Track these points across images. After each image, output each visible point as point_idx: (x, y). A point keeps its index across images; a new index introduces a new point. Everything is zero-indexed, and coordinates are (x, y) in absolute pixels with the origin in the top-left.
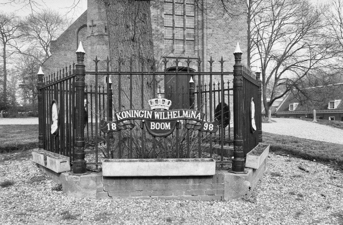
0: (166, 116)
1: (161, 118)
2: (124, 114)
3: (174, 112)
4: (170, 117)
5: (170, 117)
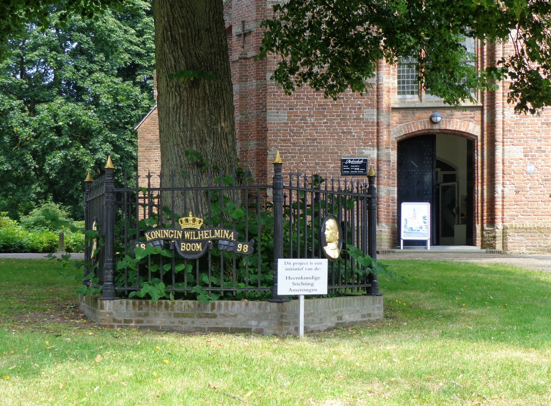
0: (197, 236)
1: (191, 239)
2: (153, 233)
3: (205, 231)
4: (201, 237)
5: (201, 237)
